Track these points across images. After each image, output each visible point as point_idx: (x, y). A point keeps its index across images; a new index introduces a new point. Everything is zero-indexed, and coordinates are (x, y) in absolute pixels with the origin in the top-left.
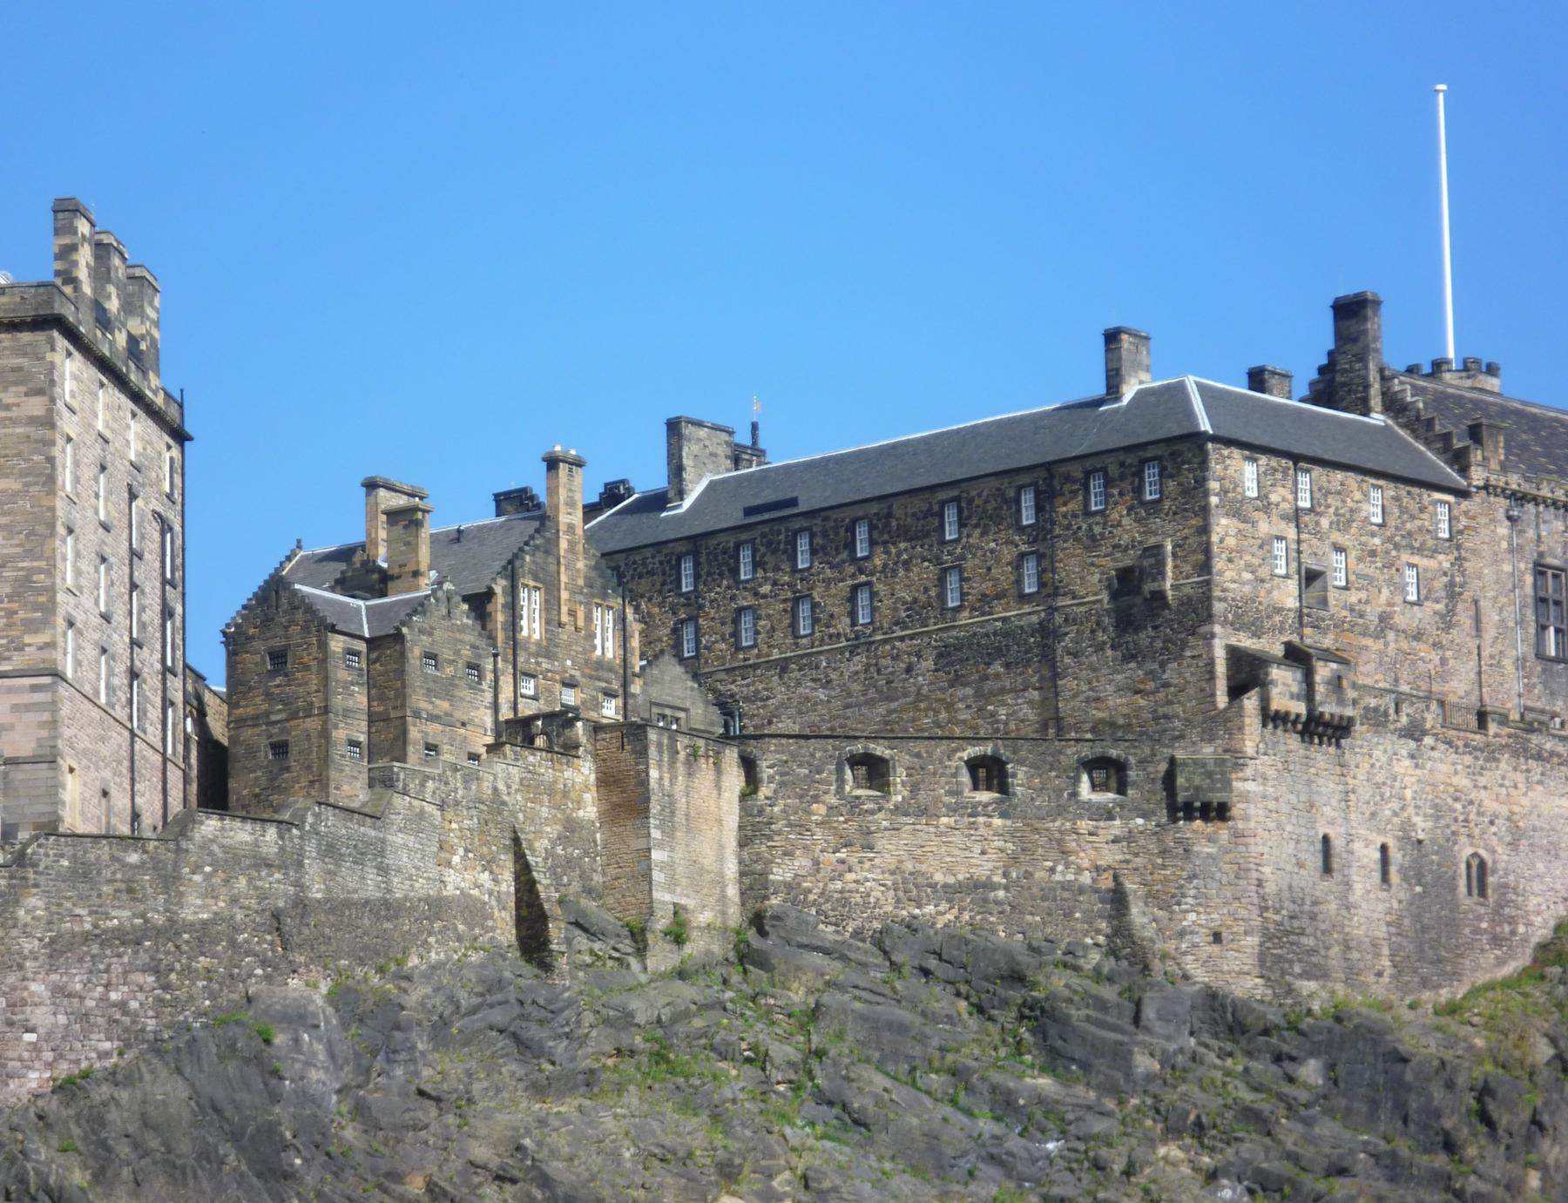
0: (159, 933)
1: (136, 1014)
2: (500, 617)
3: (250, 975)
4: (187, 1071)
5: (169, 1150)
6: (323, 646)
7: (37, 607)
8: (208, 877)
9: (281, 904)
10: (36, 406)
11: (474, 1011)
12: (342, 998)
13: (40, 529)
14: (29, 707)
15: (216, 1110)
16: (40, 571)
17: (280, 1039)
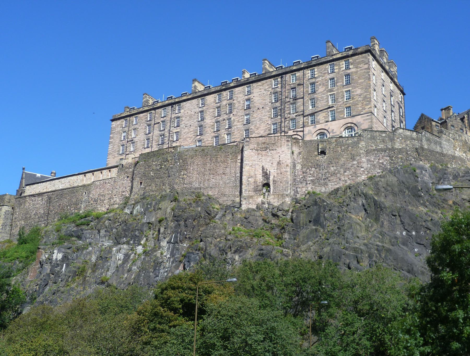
0: (390, 149)
1: (385, 165)
2: (466, 121)
3: (411, 160)
4: (397, 176)
5: (393, 190)
6: (431, 124)
7: (368, 101)
8: (401, 140)
9: (417, 147)
10: (366, 66)
11: (463, 177)
12: (433, 168)
13: (368, 87)
14: (367, 119)
15: (403, 183)
16: (368, 95)
17: (417, 171)
